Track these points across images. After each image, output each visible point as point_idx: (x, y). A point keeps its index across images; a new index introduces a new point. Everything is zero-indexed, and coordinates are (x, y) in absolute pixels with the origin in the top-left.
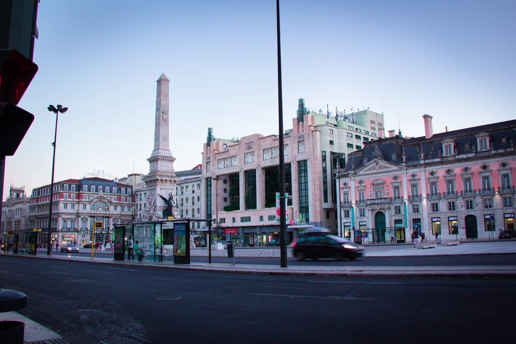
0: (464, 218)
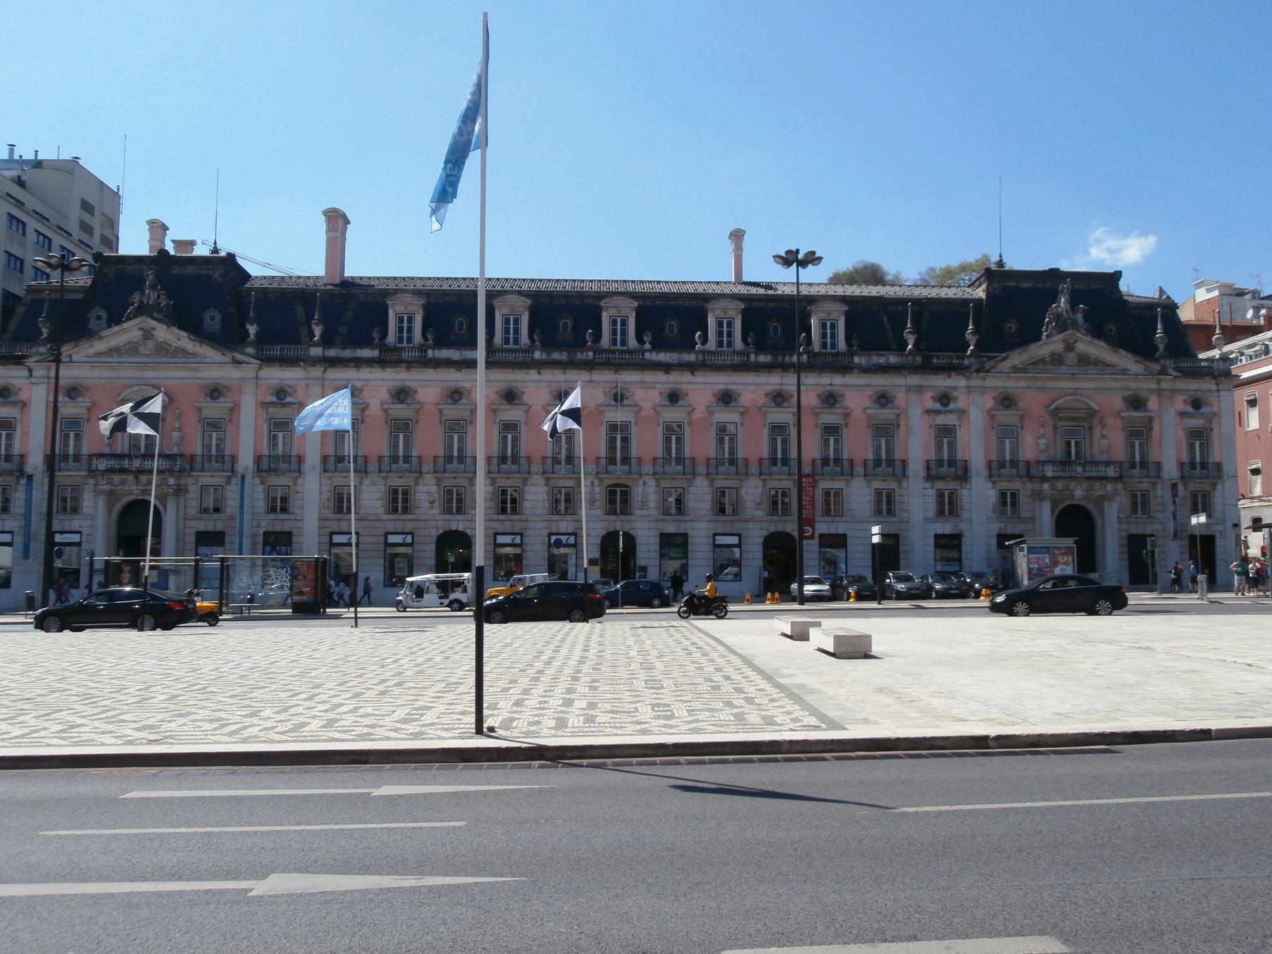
0: (434, 540)
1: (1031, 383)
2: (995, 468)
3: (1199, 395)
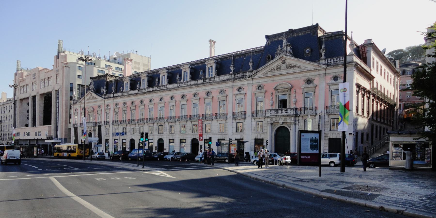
1: (269, 79)
2: (254, 114)
3: (337, 74)
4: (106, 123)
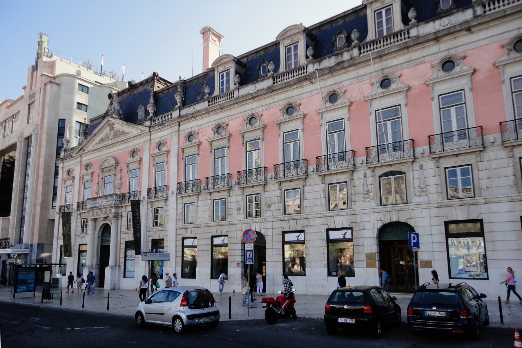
4: (154, 192)
